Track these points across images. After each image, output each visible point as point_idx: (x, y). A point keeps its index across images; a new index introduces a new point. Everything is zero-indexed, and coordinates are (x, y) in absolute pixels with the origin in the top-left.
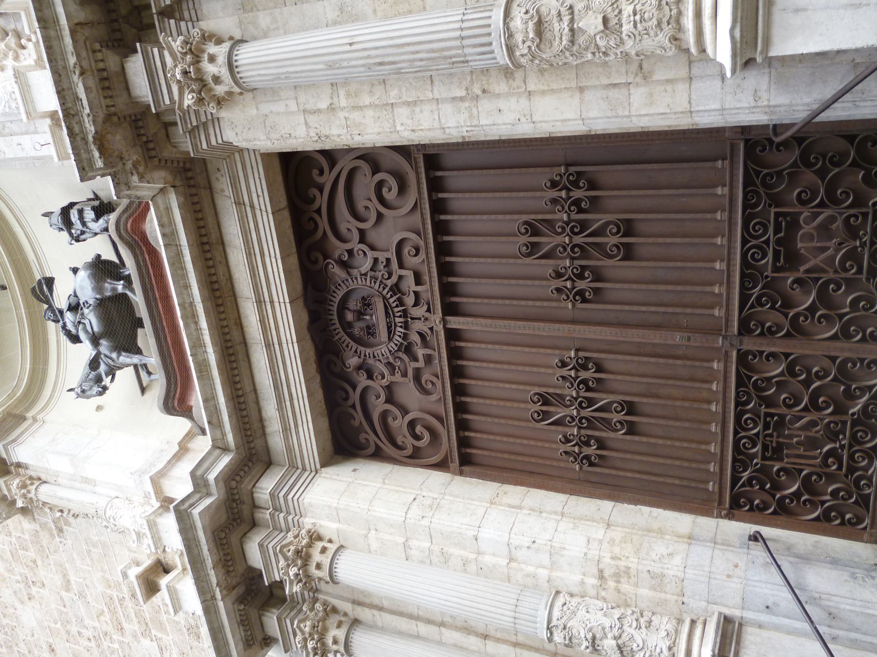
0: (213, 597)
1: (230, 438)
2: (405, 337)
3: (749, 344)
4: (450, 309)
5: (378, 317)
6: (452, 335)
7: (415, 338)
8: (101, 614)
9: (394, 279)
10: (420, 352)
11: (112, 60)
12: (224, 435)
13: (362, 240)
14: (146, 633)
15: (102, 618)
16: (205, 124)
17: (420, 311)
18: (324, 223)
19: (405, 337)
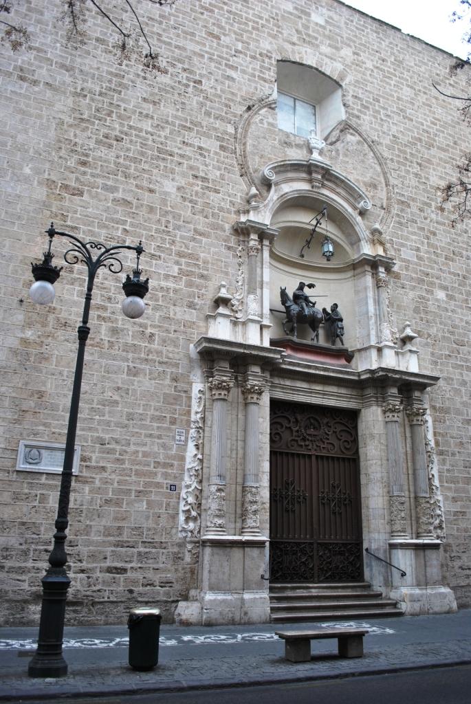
0: (245, 349)
1: (284, 366)
2: (308, 440)
3: (315, 545)
4: (317, 456)
5: (312, 431)
6: (310, 456)
7: (307, 443)
8: (185, 246)
9: (324, 440)
10: (303, 444)
11: (398, 384)
12: (285, 364)
13: (334, 432)
14: (181, 271)
15: (184, 246)
16: (377, 401)
17: (315, 447)
18: (338, 420)
19: (308, 440)
